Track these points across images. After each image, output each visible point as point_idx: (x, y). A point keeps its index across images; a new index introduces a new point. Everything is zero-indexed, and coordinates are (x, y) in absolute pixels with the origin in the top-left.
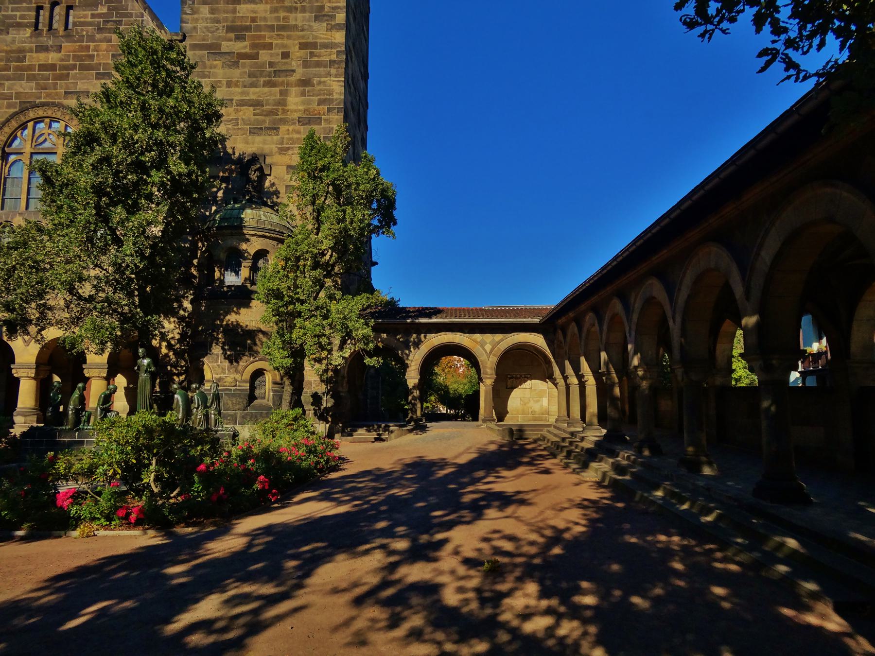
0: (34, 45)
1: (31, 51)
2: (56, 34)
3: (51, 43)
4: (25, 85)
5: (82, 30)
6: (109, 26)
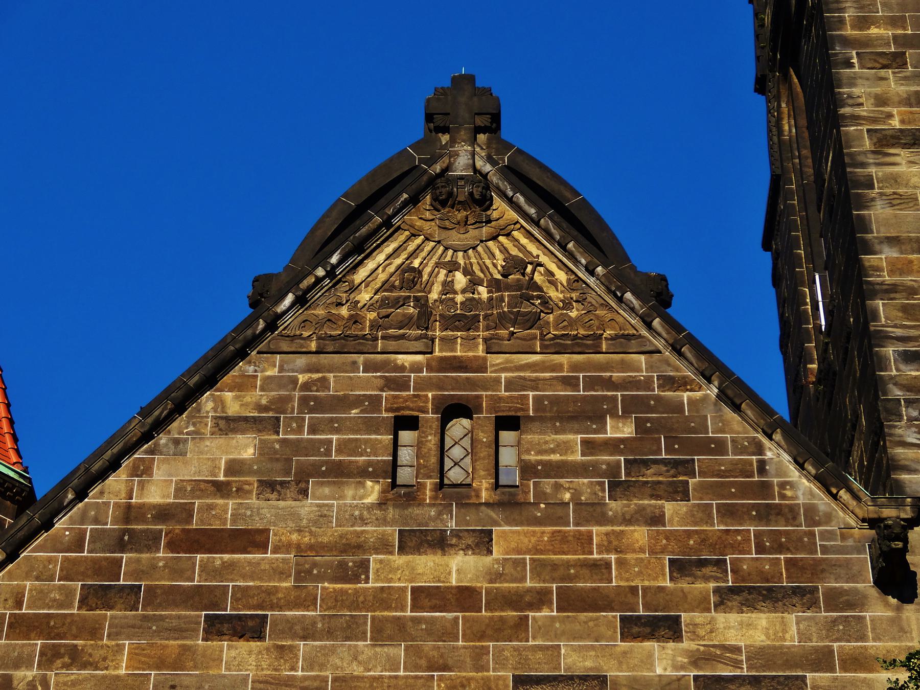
0: (392, 532)
1: (384, 546)
2: (469, 497)
3: (452, 525)
4: (369, 652)
5: (558, 487)
6: (650, 475)
